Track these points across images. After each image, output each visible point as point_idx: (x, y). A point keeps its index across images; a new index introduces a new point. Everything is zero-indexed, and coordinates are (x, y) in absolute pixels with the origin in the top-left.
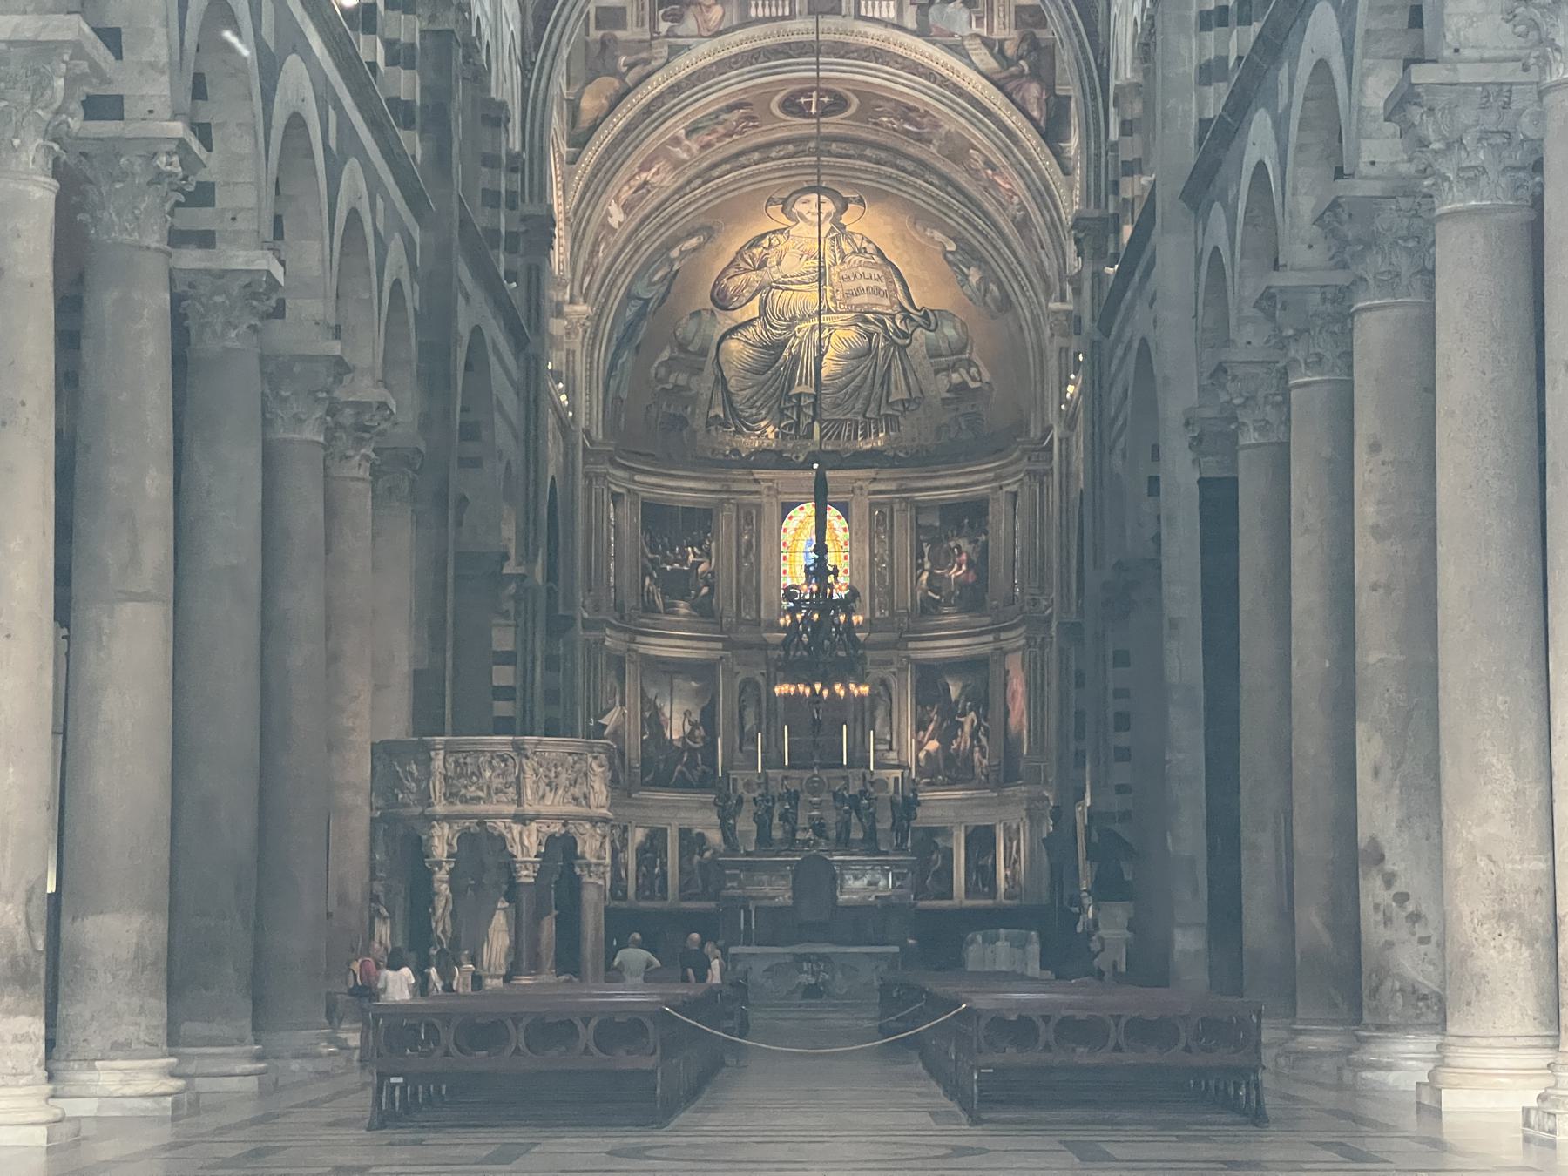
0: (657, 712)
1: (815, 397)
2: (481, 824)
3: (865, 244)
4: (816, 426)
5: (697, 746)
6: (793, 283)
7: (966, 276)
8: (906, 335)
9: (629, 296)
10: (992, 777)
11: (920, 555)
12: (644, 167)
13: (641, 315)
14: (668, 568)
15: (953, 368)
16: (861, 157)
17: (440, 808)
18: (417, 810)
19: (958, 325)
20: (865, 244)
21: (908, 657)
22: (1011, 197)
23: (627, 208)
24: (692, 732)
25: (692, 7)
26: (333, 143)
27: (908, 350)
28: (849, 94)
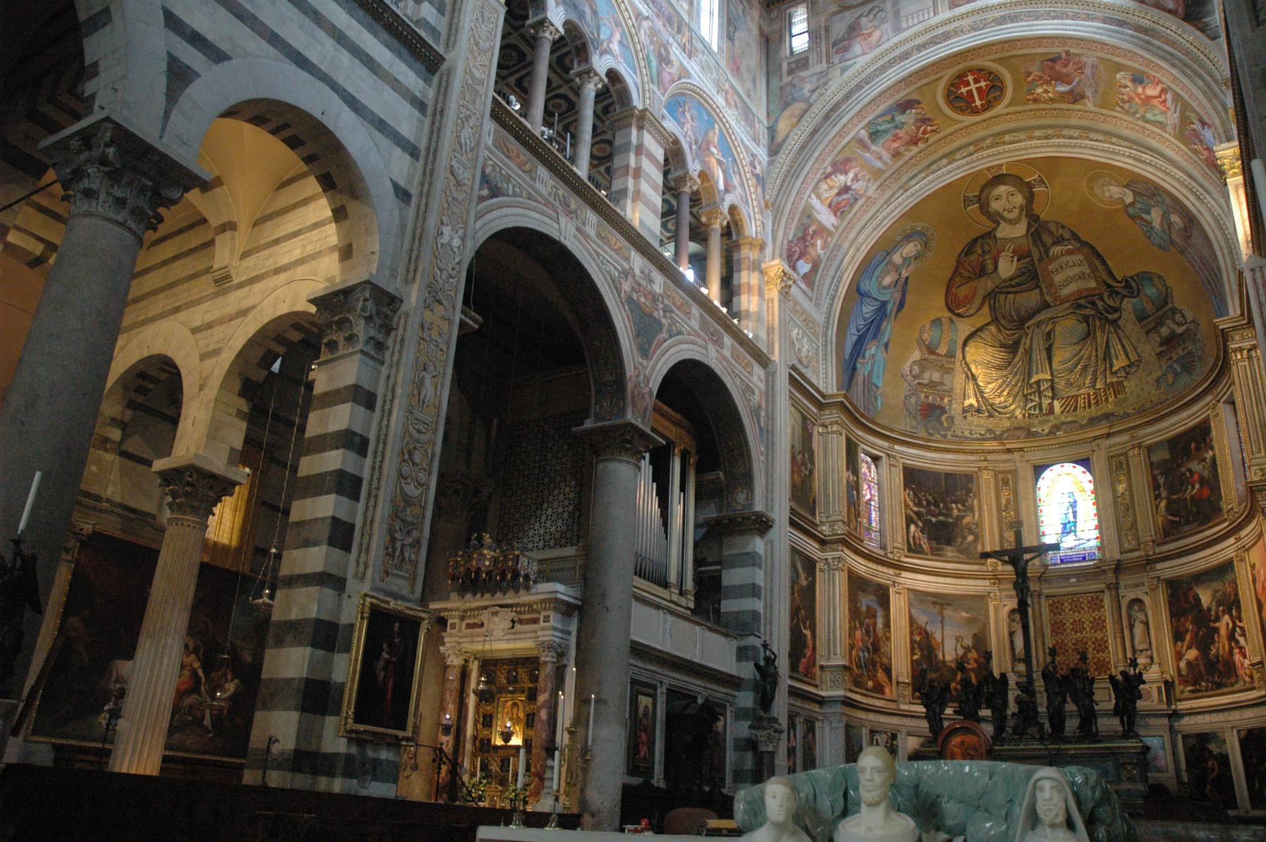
0: (927, 636)
1: (1052, 381)
3: (1060, 231)
4: (1056, 403)
5: (970, 666)
6: (1013, 286)
7: (1149, 223)
8: (1116, 310)
9: (857, 292)
10: (1256, 676)
11: (1156, 487)
12: (841, 166)
14: (934, 520)
15: (1160, 323)
16: (1031, 138)
19: (1156, 280)
20: (1060, 231)
21: (1158, 578)
22: (1164, 102)
23: (836, 209)
24: (965, 654)
25: (858, 39)
27: (1120, 322)
28: (995, 67)
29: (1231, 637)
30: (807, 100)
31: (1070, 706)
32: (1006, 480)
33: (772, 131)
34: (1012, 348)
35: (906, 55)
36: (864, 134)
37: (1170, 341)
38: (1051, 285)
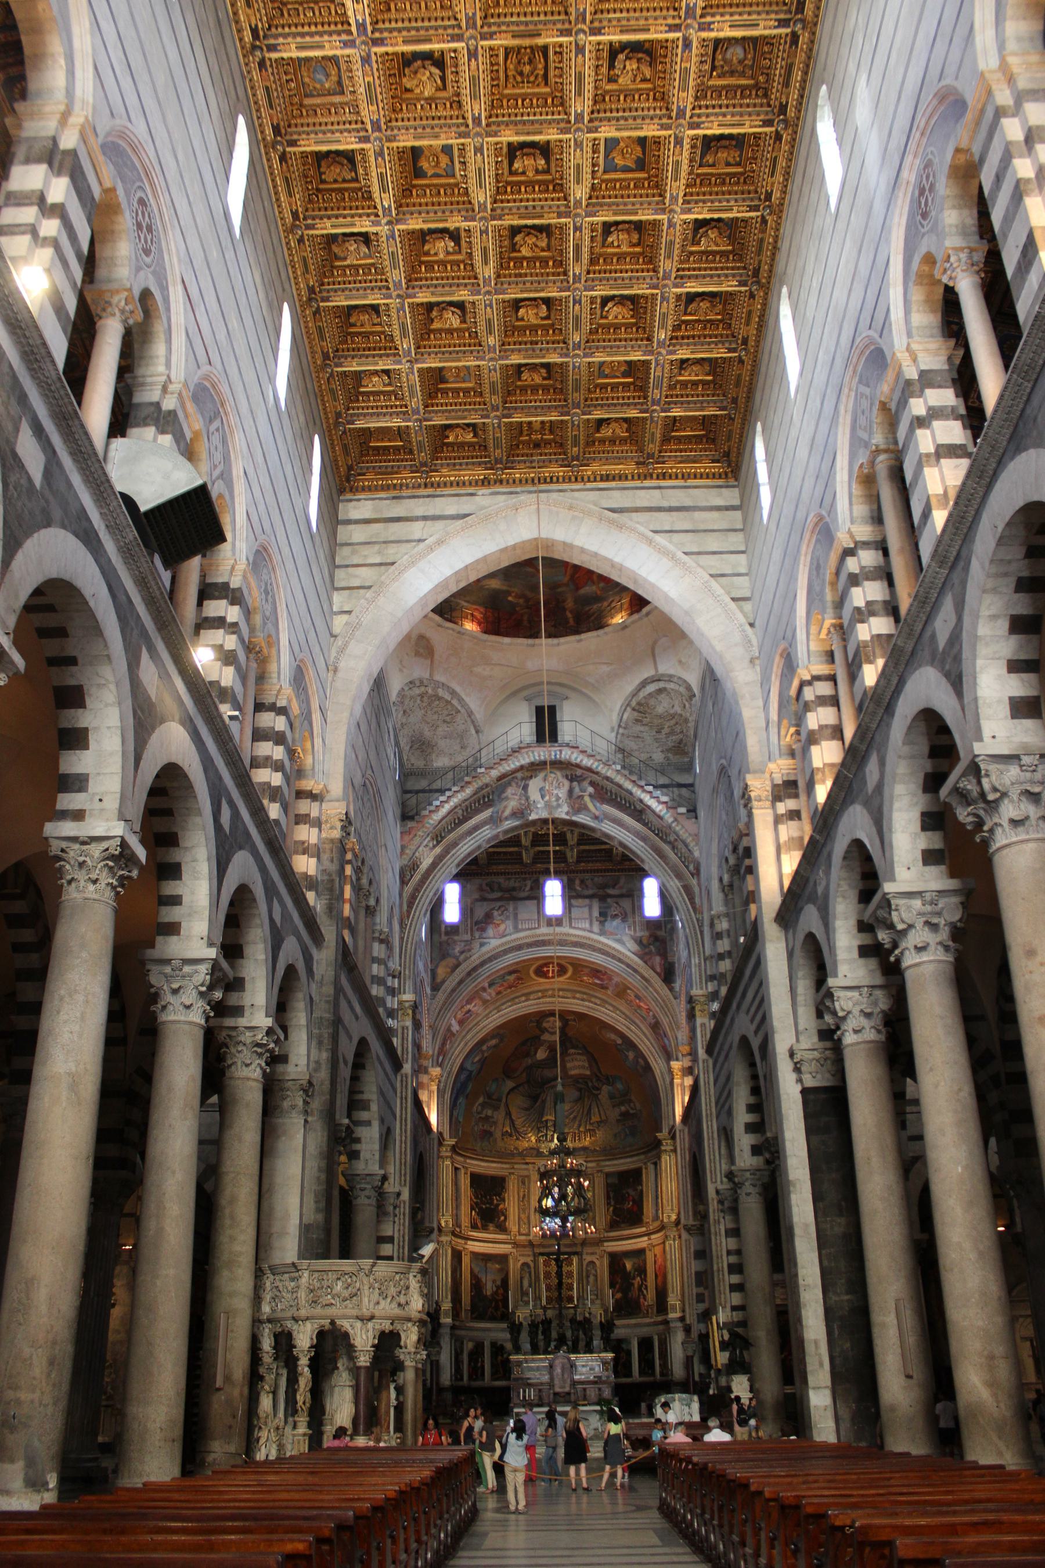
2: (333, 1323)
9: (462, 1068)
11: (608, 1197)
12: (469, 1002)
13: (469, 1078)
15: (621, 1104)
17: (303, 1313)
18: (289, 1314)
23: (461, 1023)
26: (226, 826)
29: (640, 1289)
30: (457, 958)
31: (581, 1335)
32: (524, 1180)
33: (434, 974)
34: (534, 1098)
35: (519, 948)
36: (486, 985)
37: (625, 1115)
38: (563, 1067)
